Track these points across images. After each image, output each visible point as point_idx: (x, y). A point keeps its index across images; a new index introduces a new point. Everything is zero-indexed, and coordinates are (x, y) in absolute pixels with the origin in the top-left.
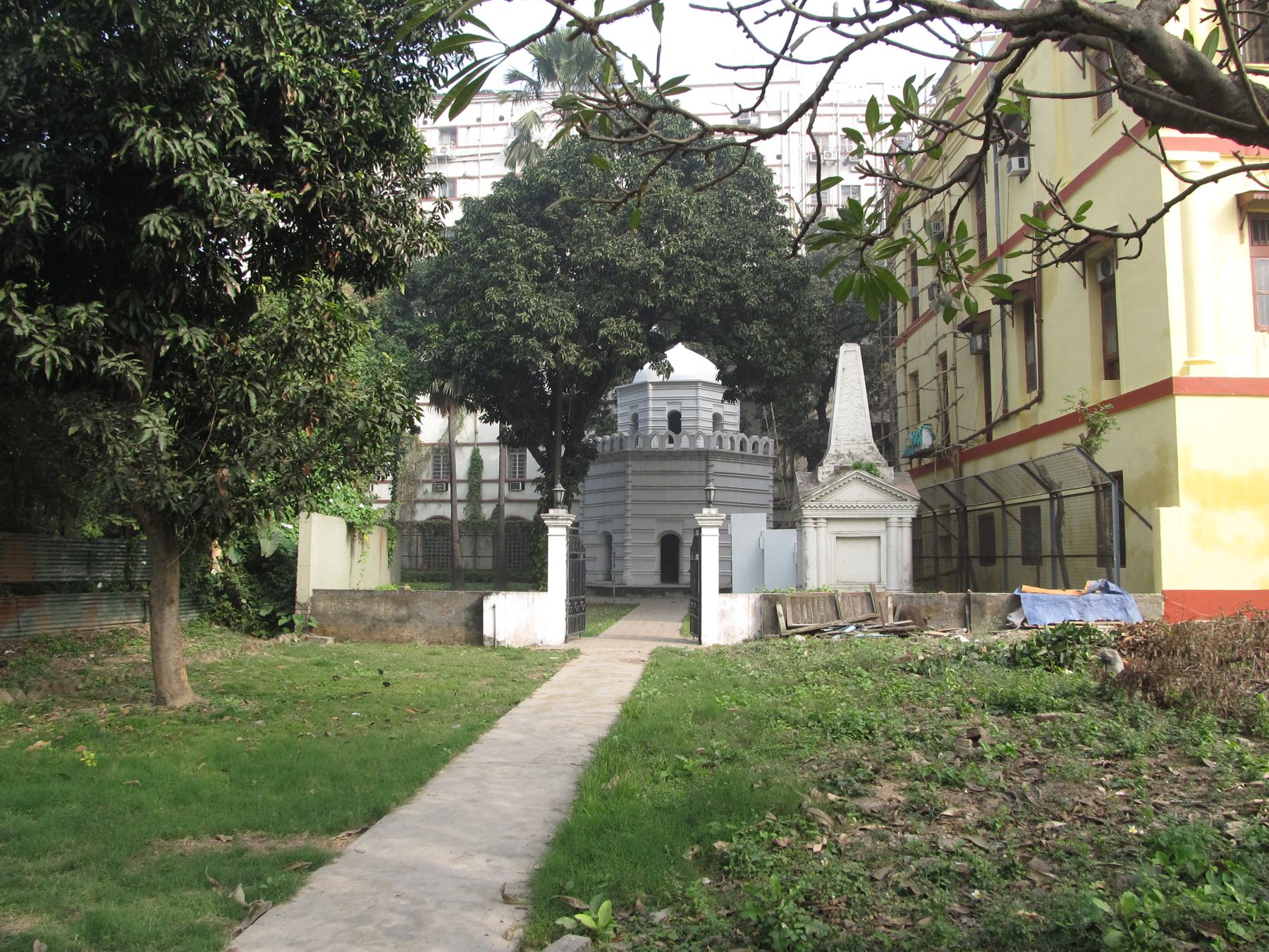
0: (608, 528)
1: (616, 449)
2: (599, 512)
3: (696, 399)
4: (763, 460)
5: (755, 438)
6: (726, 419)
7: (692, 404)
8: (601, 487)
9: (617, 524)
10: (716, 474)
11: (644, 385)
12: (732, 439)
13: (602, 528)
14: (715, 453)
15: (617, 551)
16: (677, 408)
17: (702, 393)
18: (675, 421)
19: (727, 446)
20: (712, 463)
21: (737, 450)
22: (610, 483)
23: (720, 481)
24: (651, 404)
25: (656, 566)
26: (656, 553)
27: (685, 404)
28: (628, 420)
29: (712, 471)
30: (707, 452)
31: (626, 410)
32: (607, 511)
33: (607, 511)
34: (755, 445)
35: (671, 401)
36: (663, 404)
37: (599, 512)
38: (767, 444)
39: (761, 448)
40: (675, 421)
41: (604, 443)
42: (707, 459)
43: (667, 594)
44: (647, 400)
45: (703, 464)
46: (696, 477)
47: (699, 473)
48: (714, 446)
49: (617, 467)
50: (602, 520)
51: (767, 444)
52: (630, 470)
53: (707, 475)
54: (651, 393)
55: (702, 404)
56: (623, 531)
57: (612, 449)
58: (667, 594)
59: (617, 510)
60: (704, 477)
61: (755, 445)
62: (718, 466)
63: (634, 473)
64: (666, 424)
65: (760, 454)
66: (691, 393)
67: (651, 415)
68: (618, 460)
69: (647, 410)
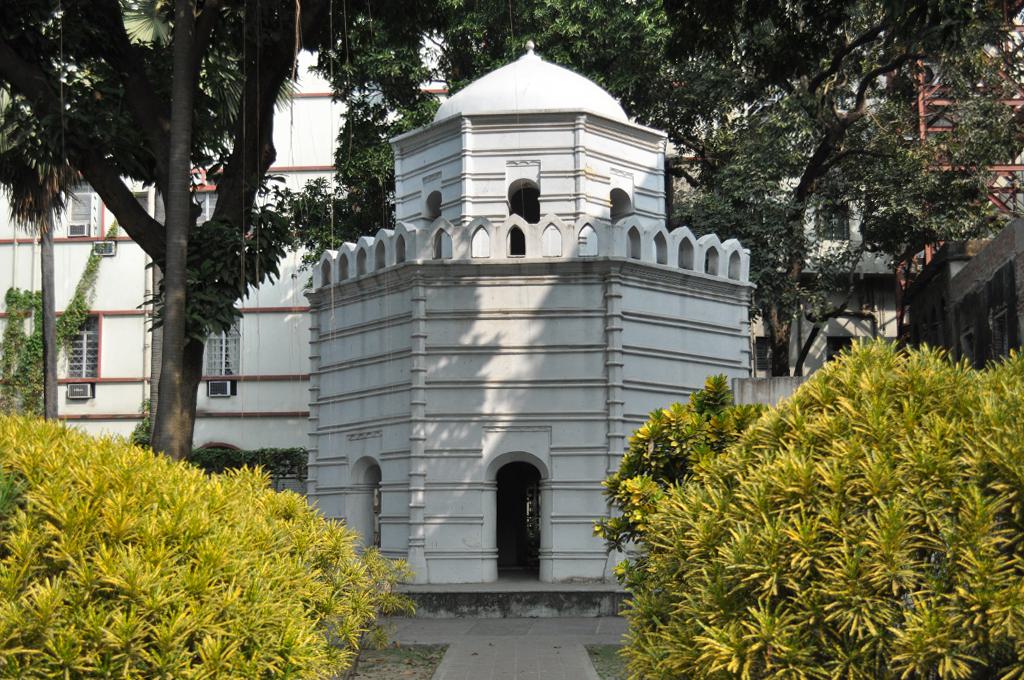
0: (373, 450)
1: (391, 262)
2: (351, 413)
3: (575, 151)
4: (726, 291)
5: (711, 239)
6: (640, 203)
7: (566, 162)
8: (356, 354)
9: (391, 439)
10: (625, 316)
11: (454, 127)
12: (660, 239)
13: (356, 451)
14: (622, 264)
15: (390, 504)
16: (530, 173)
17: (588, 139)
18: (525, 200)
19: (649, 256)
20: (615, 289)
21: (673, 264)
22: (373, 344)
23: (632, 335)
24: (470, 165)
25: (484, 537)
26: (486, 505)
27: (550, 163)
28: (420, 206)
29: (617, 307)
30: (608, 263)
31: (416, 184)
32: (371, 409)
33: (371, 409)
34: (712, 252)
35: (515, 155)
36: (498, 165)
37: (351, 413)
38: (735, 255)
39: (723, 261)
40: (525, 200)
41: (362, 253)
42: (605, 281)
43: (515, 607)
44: (460, 155)
45: (597, 293)
46: (579, 324)
47: (587, 315)
48: (620, 251)
49: (390, 305)
50: (359, 431)
51: (735, 255)
52: (421, 310)
53: (607, 318)
54: (471, 140)
55: (585, 162)
56: (406, 455)
57: (381, 264)
58: (515, 607)
59: (392, 405)
60: (598, 324)
61: (712, 252)
62: (632, 298)
63: (431, 317)
64: (504, 209)
65: (722, 276)
66: (561, 138)
67: (470, 188)
68: (397, 289)
69: (459, 179)
